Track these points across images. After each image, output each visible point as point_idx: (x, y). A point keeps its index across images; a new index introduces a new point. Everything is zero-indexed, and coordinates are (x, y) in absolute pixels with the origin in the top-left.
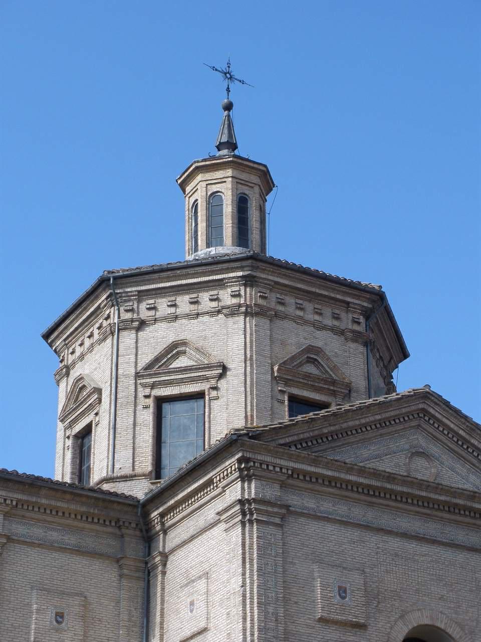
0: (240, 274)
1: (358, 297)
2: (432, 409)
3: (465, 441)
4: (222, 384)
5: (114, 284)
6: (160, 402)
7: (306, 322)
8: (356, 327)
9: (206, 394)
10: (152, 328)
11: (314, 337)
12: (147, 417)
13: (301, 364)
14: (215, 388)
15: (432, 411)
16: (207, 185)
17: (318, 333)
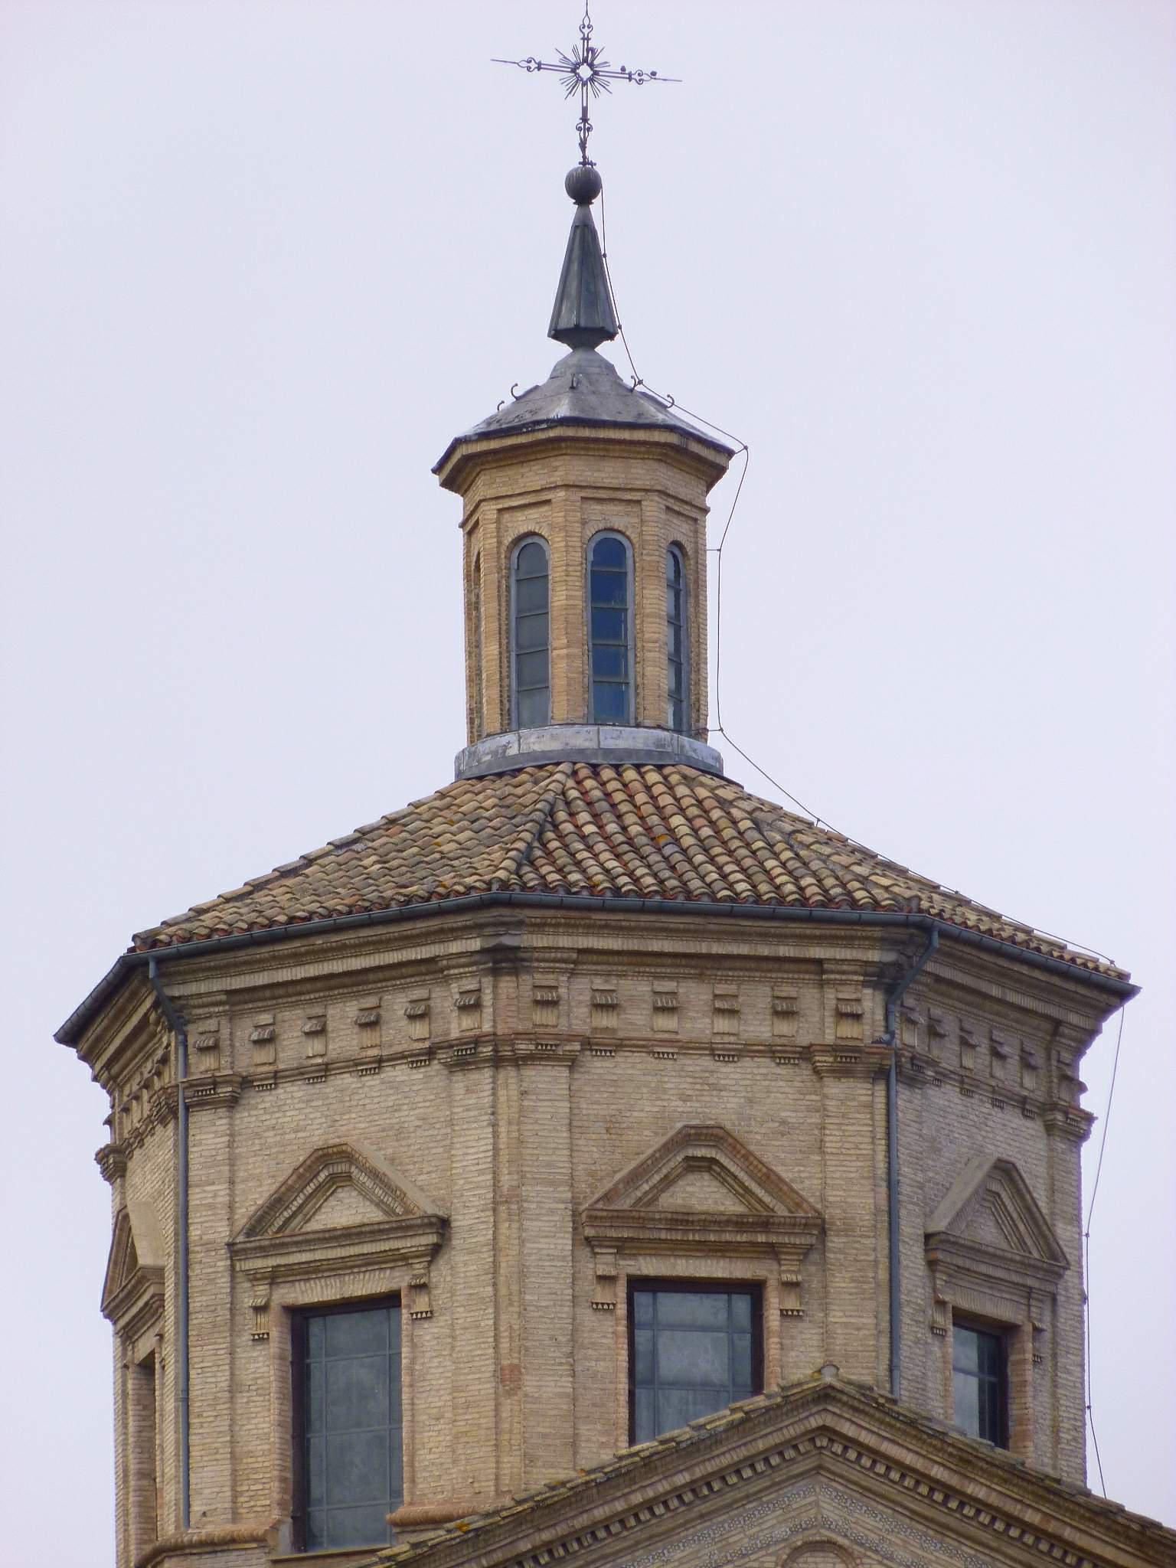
0: (475, 944)
1: (848, 941)
2: (848, 1424)
3: (950, 1492)
4: (440, 1274)
5: (160, 975)
6: (300, 1318)
7: (687, 1048)
8: (848, 1030)
9: (404, 1301)
10: (268, 1099)
11: (716, 1088)
12: (264, 1367)
13: (668, 1182)
14: (423, 1287)
15: (848, 1429)
16: (500, 511)
17: (729, 1073)
